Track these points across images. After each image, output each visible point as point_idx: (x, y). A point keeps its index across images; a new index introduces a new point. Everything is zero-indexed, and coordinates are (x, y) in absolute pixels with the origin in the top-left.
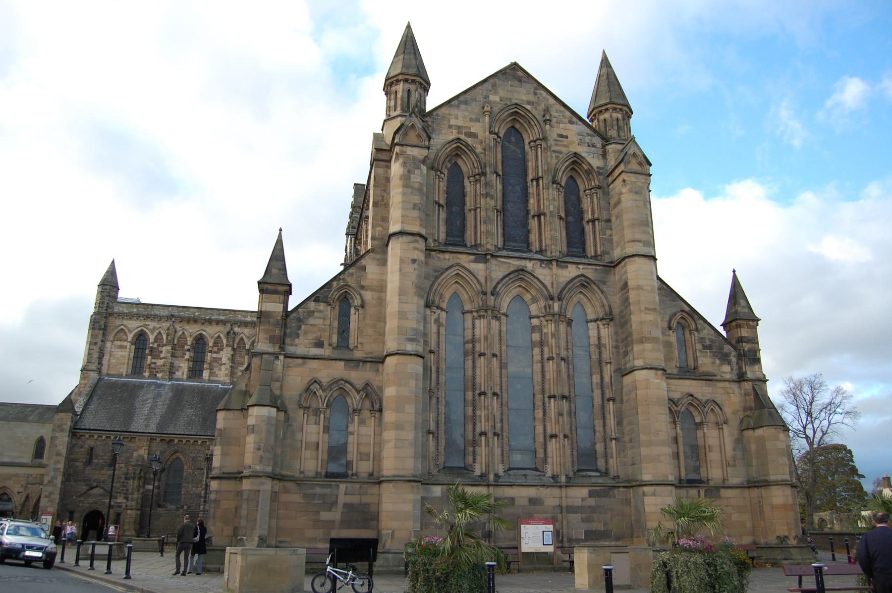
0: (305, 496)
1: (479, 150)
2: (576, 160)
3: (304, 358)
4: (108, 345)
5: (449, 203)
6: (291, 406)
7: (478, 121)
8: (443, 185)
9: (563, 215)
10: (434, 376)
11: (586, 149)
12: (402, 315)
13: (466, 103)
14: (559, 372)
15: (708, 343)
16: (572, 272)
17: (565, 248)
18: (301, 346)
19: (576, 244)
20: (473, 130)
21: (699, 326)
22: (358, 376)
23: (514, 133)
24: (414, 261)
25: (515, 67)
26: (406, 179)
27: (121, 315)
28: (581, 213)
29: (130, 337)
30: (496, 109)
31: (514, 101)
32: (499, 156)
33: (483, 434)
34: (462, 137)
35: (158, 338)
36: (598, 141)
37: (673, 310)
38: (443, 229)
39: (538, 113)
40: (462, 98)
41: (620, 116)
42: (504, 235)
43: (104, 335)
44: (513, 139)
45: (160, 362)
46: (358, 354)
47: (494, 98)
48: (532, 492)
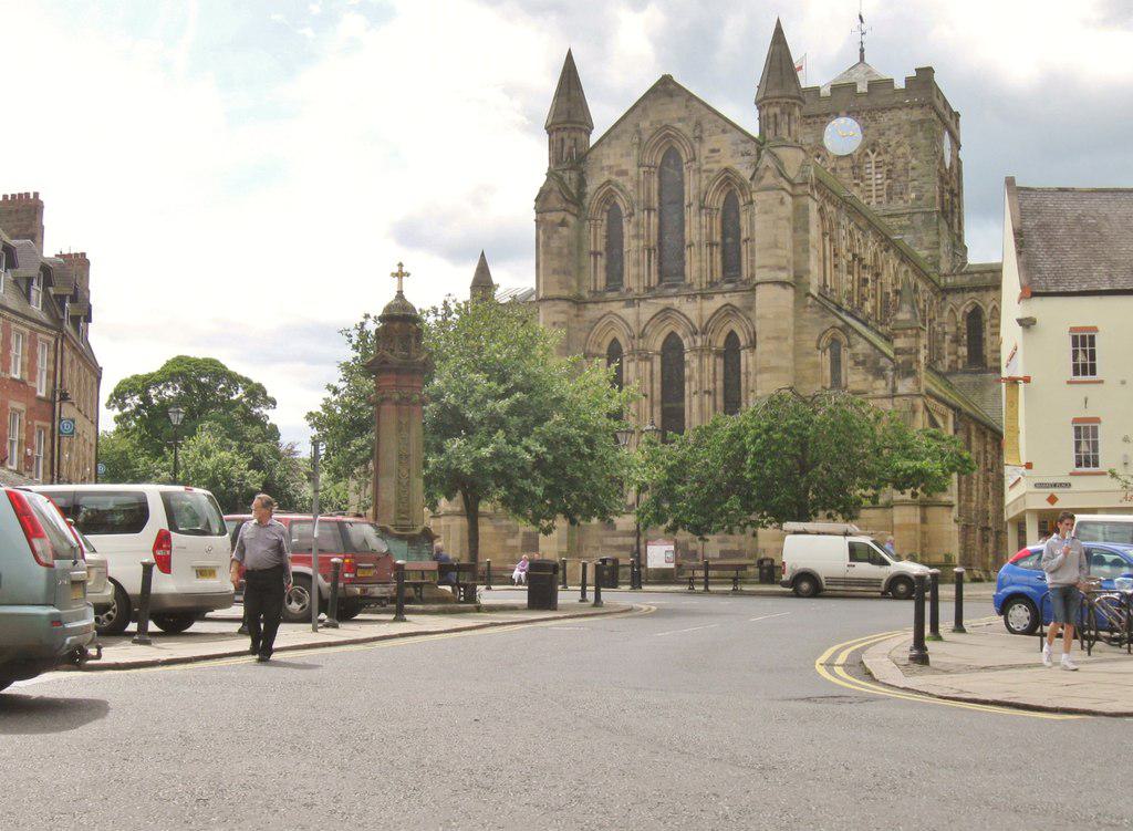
0: (496, 527)
1: (629, 187)
2: (728, 179)
5: (609, 247)
7: (628, 155)
8: (602, 232)
9: (717, 238)
13: (617, 137)
14: (701, 406)
15: (861, 358)
16: (718, 301)
17: (718, 274)
20: (624, 167)
21: (853, 341)
23: (672, 156)
24: (554, 324)
25: (666, 81)
28: (739, 231)
30: (645, 137)
31: (664, 123)
32: (655, 186)
34: (614, 177)
37: (826, 327)
39: (686, 129)
40: (613, 134)
41: (777, 110)
42: (660, 272)
44: (672, 162)
47: (645, 124)
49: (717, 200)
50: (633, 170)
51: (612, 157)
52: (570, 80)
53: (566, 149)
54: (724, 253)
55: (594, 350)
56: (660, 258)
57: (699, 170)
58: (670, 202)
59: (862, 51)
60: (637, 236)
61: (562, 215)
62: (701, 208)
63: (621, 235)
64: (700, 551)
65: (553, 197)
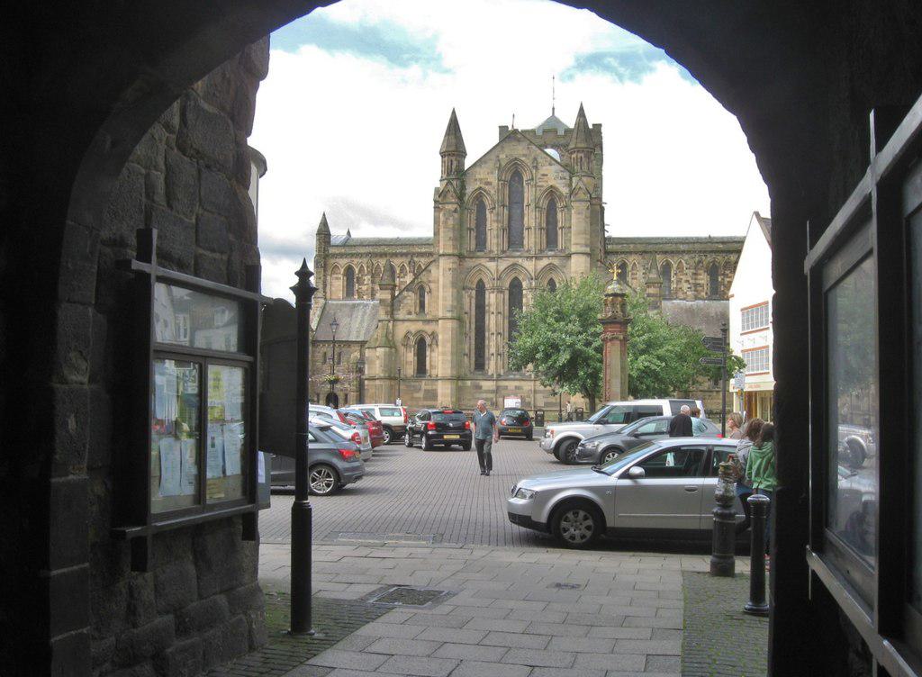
0: (407, 386)
1: (493, 192)
2: (552, 193)
3: (403, 321)
4: (329, 278)
5: (478, 226)
6: (399, 344)
7: (492, 173)
8: (474, 216)
9: (544, 225)
10: (468, 326)
11: (559, 181)
12: (445, 299)
13: (485, 162)
16: (544, 262)
18: (401, 315)
19: (551, 241)
22: (429, 328)
23: (517, 175)
24: (450, 269)
26: (445, 222)
27: (334, 256)
28: (556, 222)
29: (342, 270)
30: (503, 164)
32: (507, 192)
33: (493, 354)
34: (483, 186)
35: (361, 270)
36: (566, 175)
38: (473, 242)
39: (528, 162)
41: (582, 155)
42: (509, 242)
43: (325, 271)
44: (517, 178)
45: (364, 288)
46: (428, 317)
47: (502, 156)
48: (517, 383)
49: (544, 204)
50: (495, 182)
51: (482, 173)
52: (454, 128)
53: (454, 167)
54: (547, 234)
55: (469, 285)
56: (509, 233)
57: (536, 186)
58: (514, 201)
59: (553, 109)
60: (497, 221)
61: (455, 206)
62: (536, 208)
63: (486, 219)
64: (532, 403)
65: (449, 195)
